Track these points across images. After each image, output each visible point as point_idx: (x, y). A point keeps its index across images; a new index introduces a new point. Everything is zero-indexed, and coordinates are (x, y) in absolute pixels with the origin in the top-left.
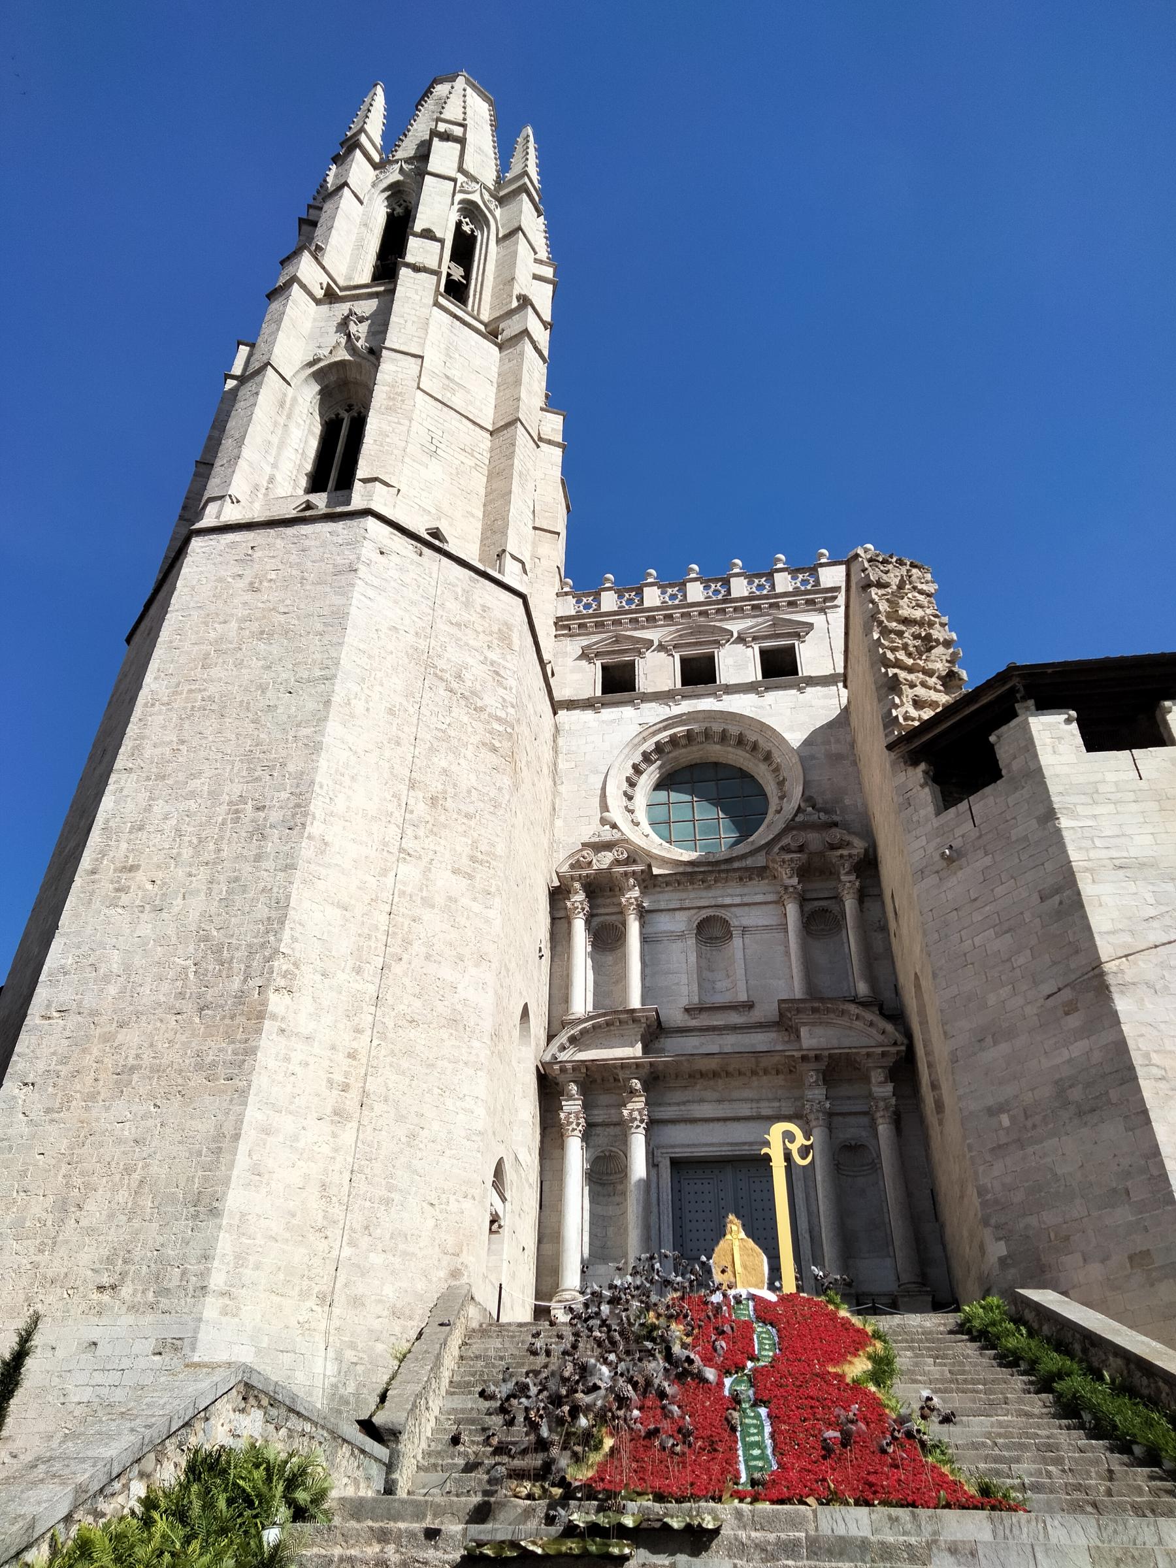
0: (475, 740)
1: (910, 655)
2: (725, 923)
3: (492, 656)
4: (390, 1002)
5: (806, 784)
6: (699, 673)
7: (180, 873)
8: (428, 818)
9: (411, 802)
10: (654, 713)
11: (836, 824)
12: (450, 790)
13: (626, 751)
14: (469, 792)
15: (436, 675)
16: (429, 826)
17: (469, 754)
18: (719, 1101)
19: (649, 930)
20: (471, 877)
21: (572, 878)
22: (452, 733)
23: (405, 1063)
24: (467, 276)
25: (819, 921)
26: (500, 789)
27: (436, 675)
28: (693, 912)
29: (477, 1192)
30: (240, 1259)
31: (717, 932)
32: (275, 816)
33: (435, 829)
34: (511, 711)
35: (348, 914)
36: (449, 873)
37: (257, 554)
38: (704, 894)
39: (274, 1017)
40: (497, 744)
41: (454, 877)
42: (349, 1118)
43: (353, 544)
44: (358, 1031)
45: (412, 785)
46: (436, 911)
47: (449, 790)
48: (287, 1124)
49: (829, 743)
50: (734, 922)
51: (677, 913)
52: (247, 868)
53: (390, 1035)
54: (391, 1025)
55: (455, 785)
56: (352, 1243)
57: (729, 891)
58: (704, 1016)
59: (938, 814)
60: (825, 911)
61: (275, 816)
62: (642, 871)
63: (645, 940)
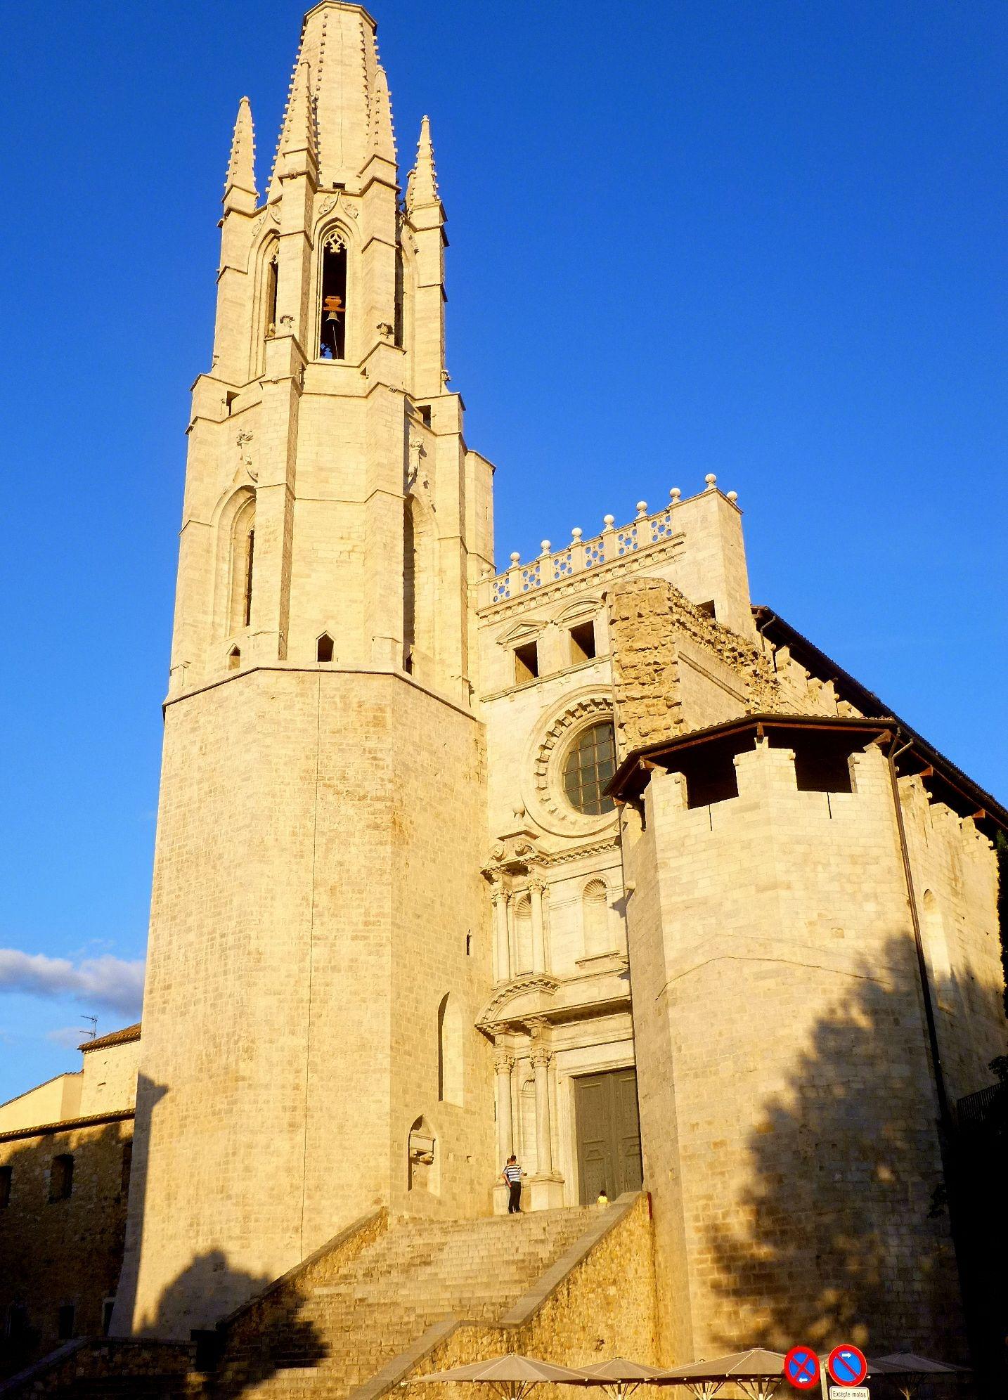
0: (361, 825)
3: (370, 744)
4: (316, 1045)
7: (190, 987)
9: (316, 898)
12: (345, 876)
15: (325, 785)
17: (357, 840)
18: (595, 1034)
20: (366, 938)
22: (341, 829)
23: (331, 1084)
24: (343, 305)
27: (325, 785)
29: (388, 1150)
30: (246, 1218)
31: (599, 890)
32: (230, 940)
34: (389, 786)
35: (281, 997)
37: (202, 720)
39: (243, 1079)
40: (379, 821)
42: (299, 1126)
44: (297, 1072)
45: (315, 885)
48: (261, 1139)
52: (221, 979)
53: (320, 1068)
54: (318, 1060)
56: (310, 1197)
57: (605, 856)
61: (230, 940)
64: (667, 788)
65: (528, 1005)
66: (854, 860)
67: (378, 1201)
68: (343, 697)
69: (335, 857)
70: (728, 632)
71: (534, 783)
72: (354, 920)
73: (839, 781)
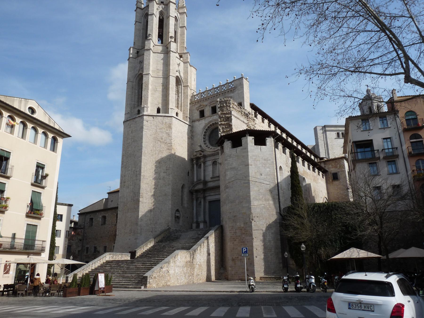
1: (225, 121)
3: (167, 132)
6: (214, 110)
7: (129, 182)
24: (163, 31)
30: (141, 229)
32: (138, 173)
43: (142, 122)
61: (138, 173)
64: (227, 144)
65: (200, 186)
66: (265, 160)
67: (168, 226)
68: (162, 121)
70: (244, 109)
71: (203, 140)
73: (264, 143)
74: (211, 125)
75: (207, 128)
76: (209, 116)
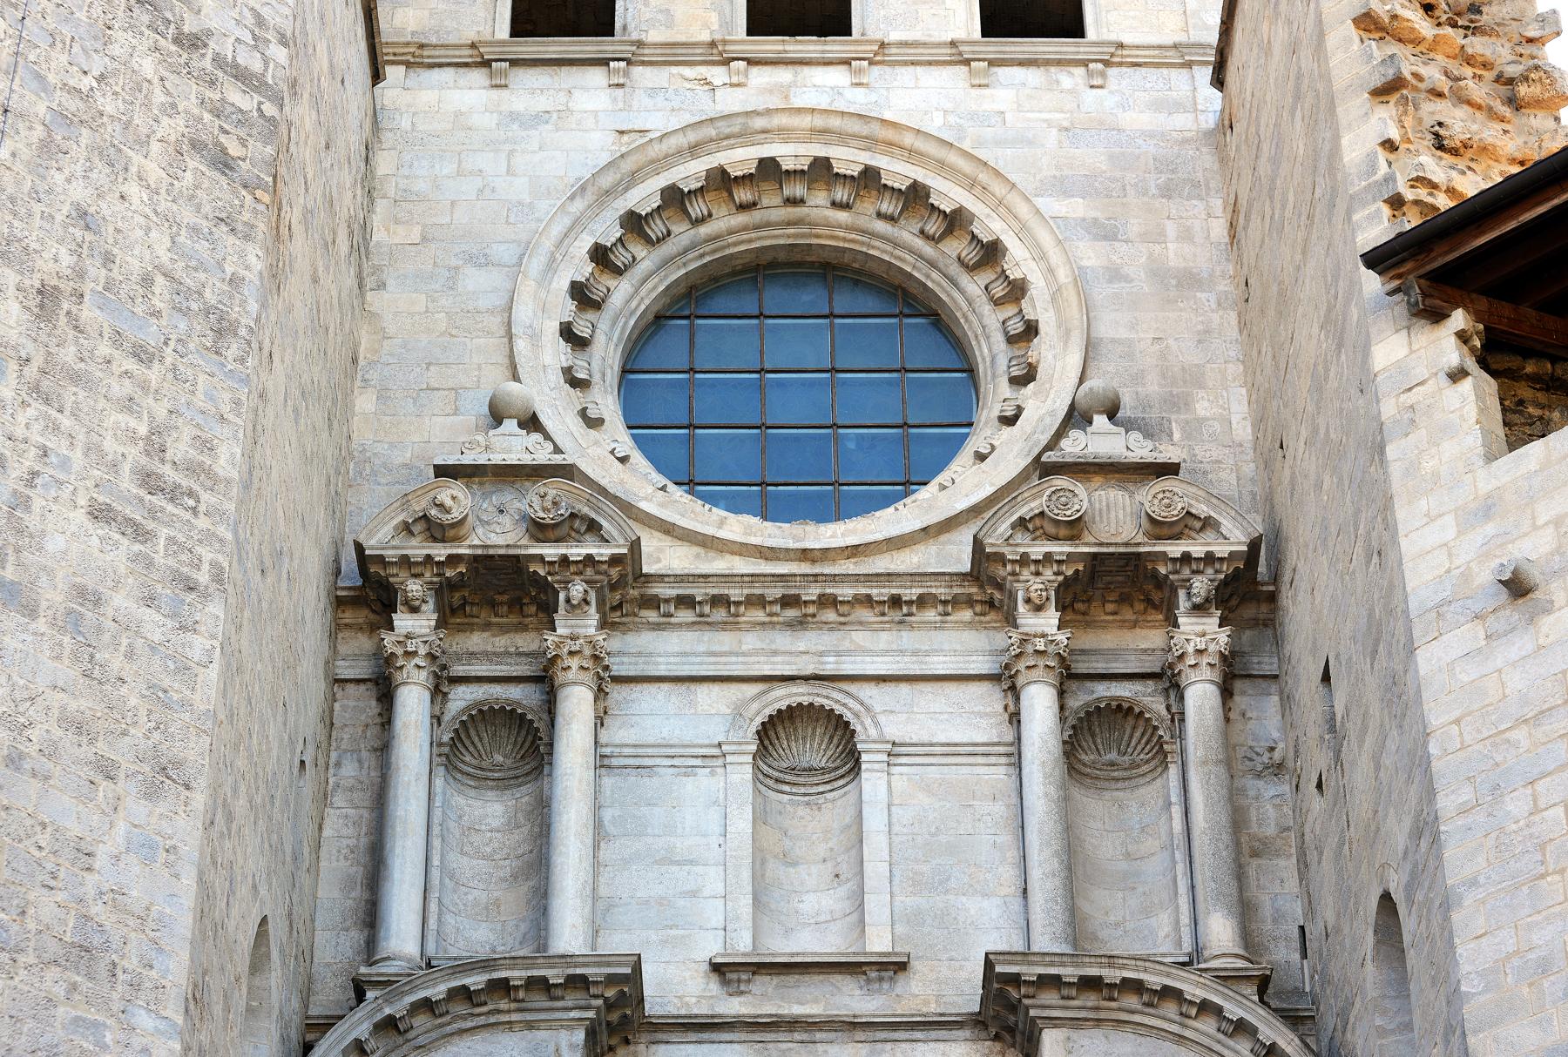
0: (173, 127)
2: (840, 729)
5: (1091, 349)
8: (29, 348)
10: (664, 104)
11: (1170, 469)
12: (95, 270)
13: (578, 206)
14: (147, 281)
16: (31, 371)
17: (155, 172)
19: (616, 734)
20: (141, 534)
21: (405, 561)
22: (109, 105)
25: (1109, 736)
26: (235, 281)
28: (752, 689)
31: (812, 750)
33: (46, 384)
34: (279, 54)
36: (80, 516)
38: (783, 640)
40: (234, 149)
41: (102, 530)
46: (41, 625)
47: (92, 272)
49: (1159, 237)
50: (865, 732)
51: (704, 692)
55: (108, 259)
57: (860, 637)
58: (763, 984)
59: (1490, 458)
60: (1123, 712)
62: (615, 560)
63: (603, 762)
69: (72, 186)
71: (557, 353)
72: (109, 445)
74: (721, 181)
75: (643, 197)
76: (717, 54)
